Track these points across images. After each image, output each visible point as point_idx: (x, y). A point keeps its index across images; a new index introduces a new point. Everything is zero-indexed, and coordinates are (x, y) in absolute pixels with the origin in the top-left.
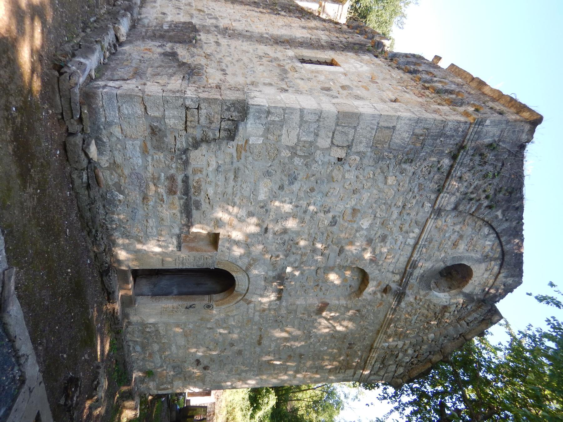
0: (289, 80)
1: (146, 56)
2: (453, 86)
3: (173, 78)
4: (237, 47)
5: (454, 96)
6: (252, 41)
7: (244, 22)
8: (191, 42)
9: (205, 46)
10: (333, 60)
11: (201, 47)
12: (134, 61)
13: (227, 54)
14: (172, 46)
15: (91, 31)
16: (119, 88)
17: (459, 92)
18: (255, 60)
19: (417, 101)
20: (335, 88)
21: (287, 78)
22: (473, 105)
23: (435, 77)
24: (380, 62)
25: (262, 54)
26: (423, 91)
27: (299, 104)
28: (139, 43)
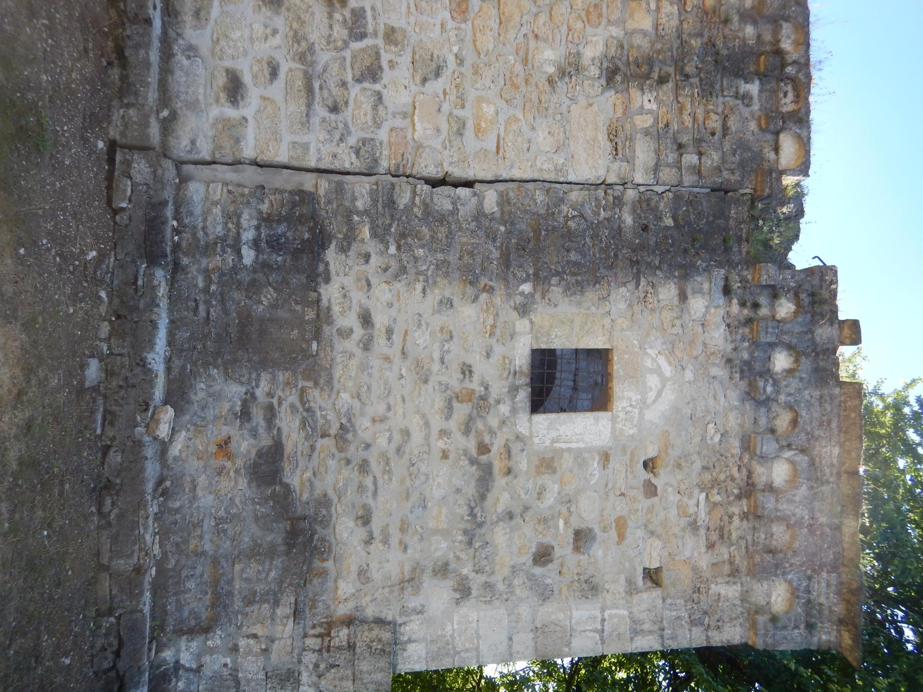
0: (483, 531)
1: (225, 485)
2: (803, 491)
3: (279, 612)
4: (409, 347)
5: (778, 530)
6: (447, 275)
7: (451, 59)
8: (306, 354)
9: (341, 345)
10: (612, 350)
11: (330, 382)
12: (205, 527)
13: (381, 408)
14: (270, 395)
15: (113, 504)
16: (198, 670)
17: (796, 522)
18: (437, 422)
19: (695, 569)
20: (563, 551)
21: (480, 525)
22: (790, 582)
23: (789, 446)
24: (718, 337)
25: (454, 380)
26: (735, 509)
27: (477, 649)
28: (199, 391)
